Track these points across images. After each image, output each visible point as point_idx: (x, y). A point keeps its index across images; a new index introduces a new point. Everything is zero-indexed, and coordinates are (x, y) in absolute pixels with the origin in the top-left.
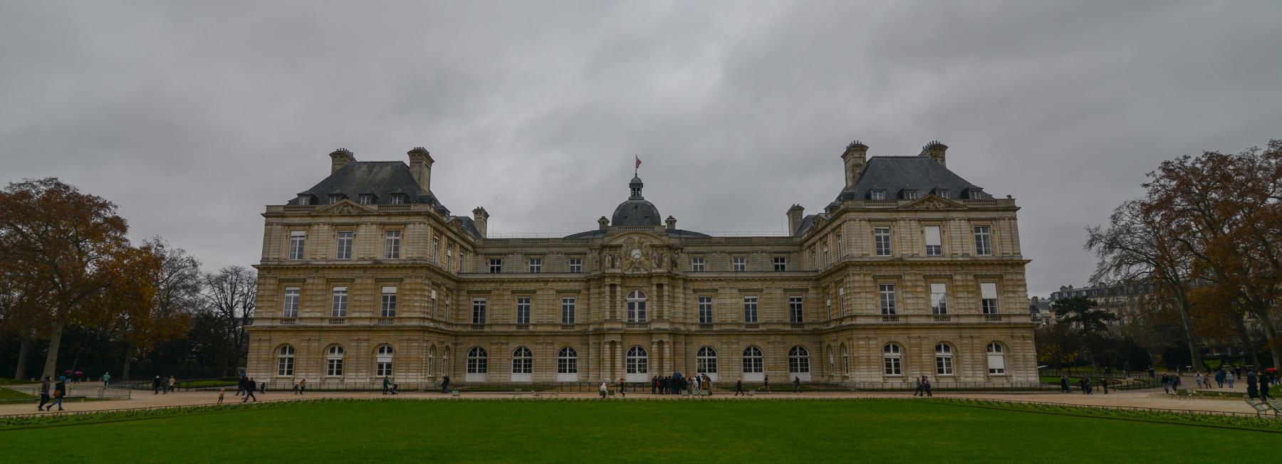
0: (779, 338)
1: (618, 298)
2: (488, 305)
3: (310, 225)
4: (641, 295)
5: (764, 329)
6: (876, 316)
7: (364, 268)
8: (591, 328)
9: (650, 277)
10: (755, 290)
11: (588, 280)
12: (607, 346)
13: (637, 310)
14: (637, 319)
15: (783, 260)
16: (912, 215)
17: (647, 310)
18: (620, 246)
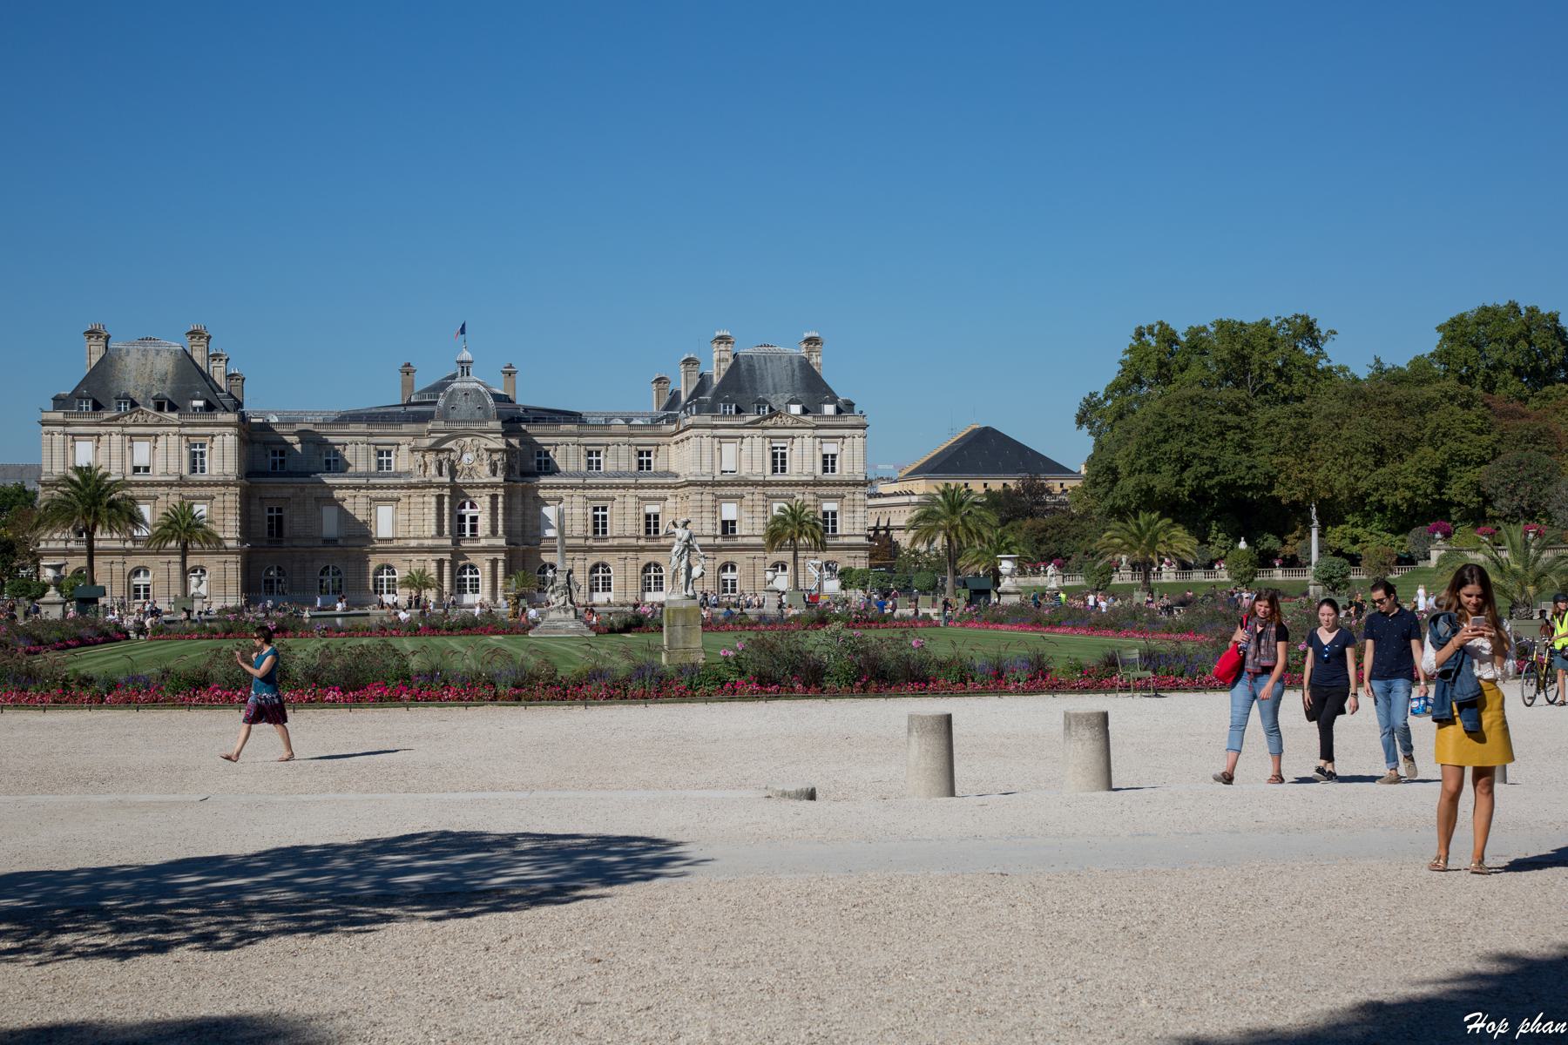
0: (630, 554)
1: (446, 511)
2: (286, 513)
3: (99, 435)
4: (473, 506)
5: (616, 542)
6: (715, 537)
7: (169, 484)
8: (413, 543)
9: (485, 486)
10: (607, 499)
11: (411, 486)
12: (434, 564)
13: (468, 523)
14: (468, 533)
15: (649, 454)
16: (759, 432)
17: (480, 523)
18: (451, 450)
